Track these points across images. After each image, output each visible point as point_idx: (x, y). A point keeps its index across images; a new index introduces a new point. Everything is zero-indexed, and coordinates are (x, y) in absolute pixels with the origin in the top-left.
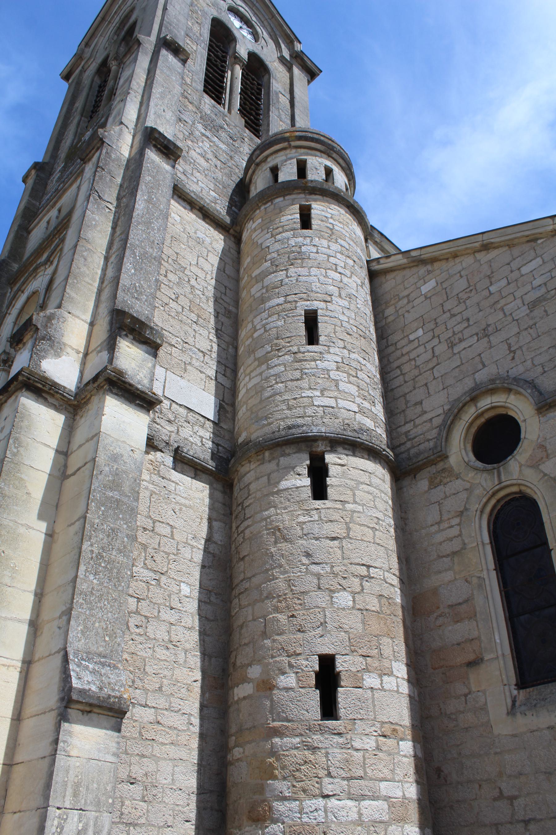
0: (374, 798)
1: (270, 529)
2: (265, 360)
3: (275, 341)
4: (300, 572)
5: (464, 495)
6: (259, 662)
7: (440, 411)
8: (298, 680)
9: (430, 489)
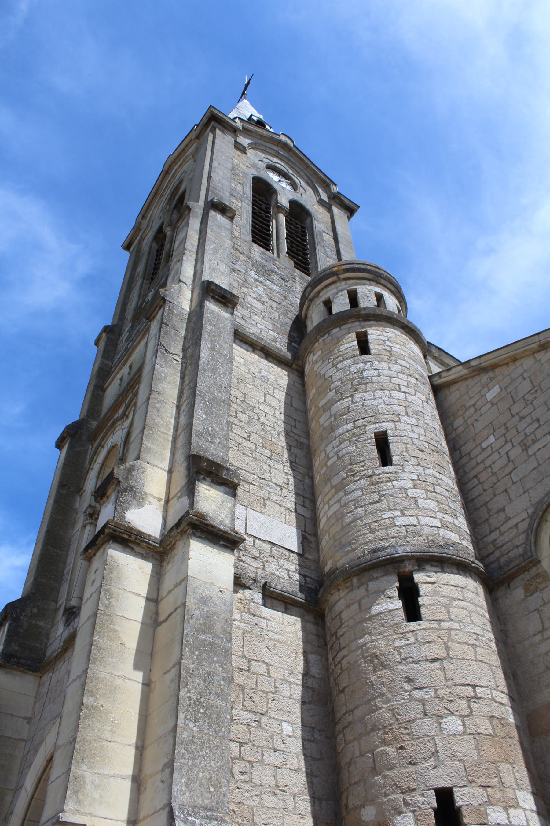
1: (367, 657)
2: (341, 486)
3: (350, 467)
4: (403, 699)
6: (372, 801)
7: (525, 515)
9: (526, 596)
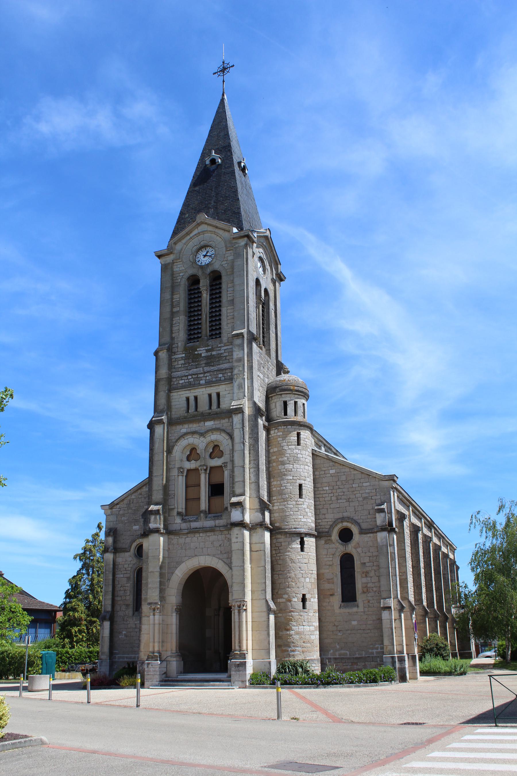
0: (312, 626)
2: (285, 500)
5: (335, 550)
7: (331, 520)
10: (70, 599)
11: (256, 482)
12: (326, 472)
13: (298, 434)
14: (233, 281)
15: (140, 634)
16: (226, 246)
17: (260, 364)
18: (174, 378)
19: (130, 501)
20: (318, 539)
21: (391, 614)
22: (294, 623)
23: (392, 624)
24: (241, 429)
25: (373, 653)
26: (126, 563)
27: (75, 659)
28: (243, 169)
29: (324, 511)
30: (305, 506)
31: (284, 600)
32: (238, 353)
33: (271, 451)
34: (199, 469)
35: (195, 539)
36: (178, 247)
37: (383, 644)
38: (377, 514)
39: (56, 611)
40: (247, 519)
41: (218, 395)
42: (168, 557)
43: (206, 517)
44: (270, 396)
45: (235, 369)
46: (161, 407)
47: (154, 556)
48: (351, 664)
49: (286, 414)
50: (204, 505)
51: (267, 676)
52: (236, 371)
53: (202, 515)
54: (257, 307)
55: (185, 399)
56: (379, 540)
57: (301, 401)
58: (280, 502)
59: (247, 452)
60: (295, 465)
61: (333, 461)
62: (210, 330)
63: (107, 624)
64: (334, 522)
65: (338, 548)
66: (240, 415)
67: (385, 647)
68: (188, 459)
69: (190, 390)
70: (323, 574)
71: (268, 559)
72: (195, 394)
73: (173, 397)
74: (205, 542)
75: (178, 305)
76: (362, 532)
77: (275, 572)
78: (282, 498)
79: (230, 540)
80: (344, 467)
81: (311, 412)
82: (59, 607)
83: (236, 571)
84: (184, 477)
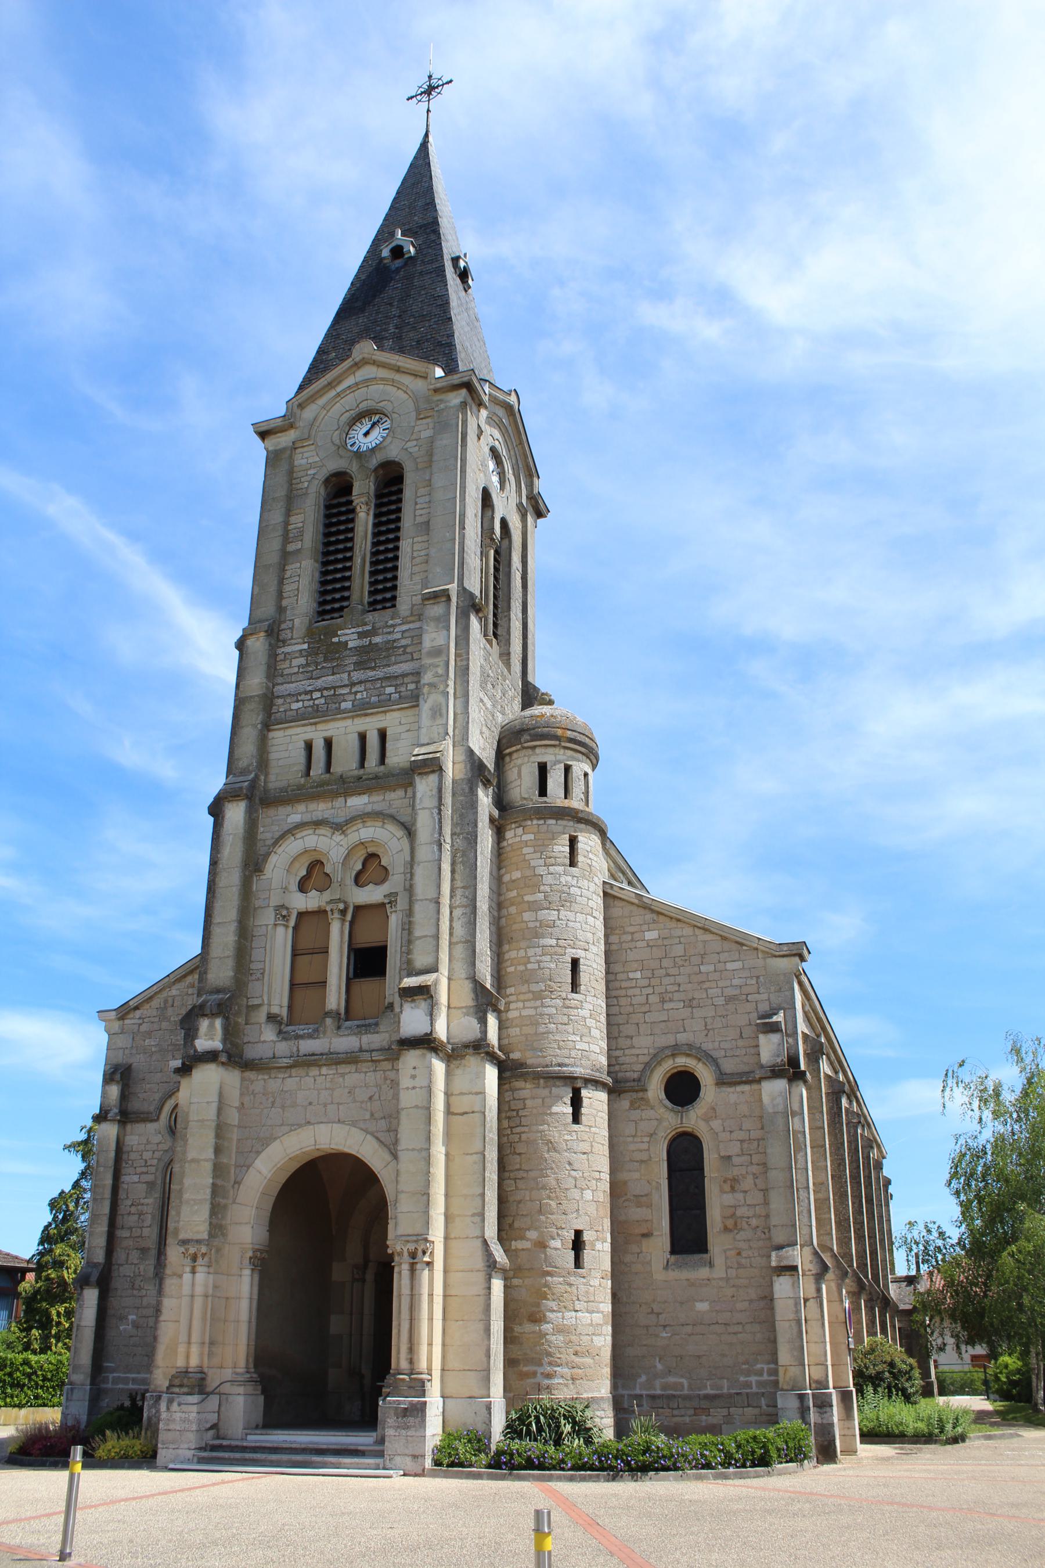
0: (598, 1312)
2: (538, 996)
6: (536, 1229)
7: (646, 1051)
8: (563, 1244)
10: (50, 1243)
11: (467, 942)
12: (637, 936)
13: (573, 841)
14: (429, 483)
15: (157, 1322)
16: (418, 411)
17: (485, 678)
18: (278, 697)
19: (166, 1001)
20: (614, 1096)
21: (795, 1285)
22: (553, 1305)
23: (798, 1311)
24: (436, 811)
25: (748, 1385)
26: (148, 1147)
27: (45, 1379)
28: (464, 275)
29: (629, 1030)
30: (585, 1013)
31: (527, 1245)
32: (434, 635)
33: (506, 878)
34: (328, 909)
35: (309, 1080)
36: (308, 413)
37: (775, 1360)
38: (761, 1037)
39: (24, 1271)
40: (441, 1031)
41: (383, 735)
42: (239, 1127)
43: (339, 1028)
44: (508, 751)
45: (425, 673)
46: (243, 763)
47: (203, 1121)
48: (692, 1412)
49: (543, 791)
50: (334, 997)
51: (479, 1441)
52: (427, 678)
53: (329, 1021)
54: (484, 554)
55: (302, 745)
56: (766, 1099)
57: (580, 767)
58: (523, 1001)
59: (446, 867)
60: (562, 912)
61: (653, 911)
62: (370, 592)
63: (91, 1296)
64: (655, 1055)
65: (663, 1120)
66: (433, 778)
67: (781, 1370)
68: (303, 887)
69: (315, 724)
70: (625, 1183)
71: (492, 1135)
72: (328, 734)
73: (275, 742)
74: (333, 1090)
75: (300, 536)
76: (723, 1080)
77: (507, 1174)
78: (530, 992)
79: (395, 1084)
80: (680, 925)
81: (601, 790)
82: (28, 1262)
83: (407, 1161)
84: (290, 930)
